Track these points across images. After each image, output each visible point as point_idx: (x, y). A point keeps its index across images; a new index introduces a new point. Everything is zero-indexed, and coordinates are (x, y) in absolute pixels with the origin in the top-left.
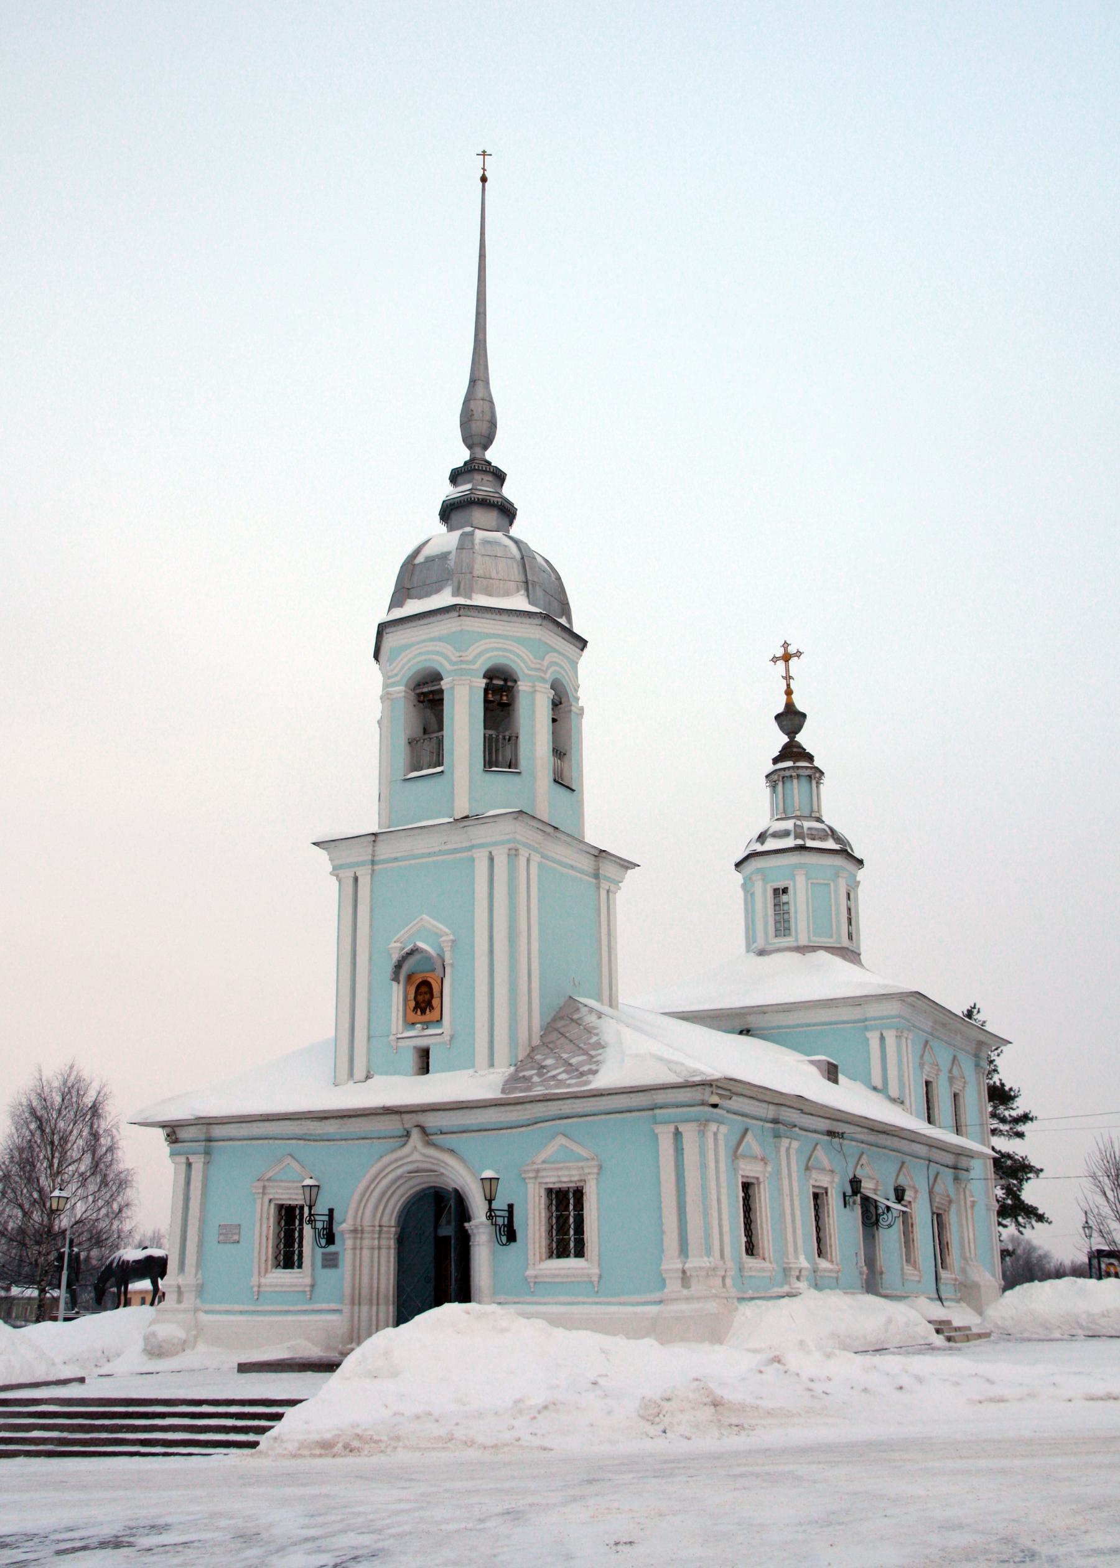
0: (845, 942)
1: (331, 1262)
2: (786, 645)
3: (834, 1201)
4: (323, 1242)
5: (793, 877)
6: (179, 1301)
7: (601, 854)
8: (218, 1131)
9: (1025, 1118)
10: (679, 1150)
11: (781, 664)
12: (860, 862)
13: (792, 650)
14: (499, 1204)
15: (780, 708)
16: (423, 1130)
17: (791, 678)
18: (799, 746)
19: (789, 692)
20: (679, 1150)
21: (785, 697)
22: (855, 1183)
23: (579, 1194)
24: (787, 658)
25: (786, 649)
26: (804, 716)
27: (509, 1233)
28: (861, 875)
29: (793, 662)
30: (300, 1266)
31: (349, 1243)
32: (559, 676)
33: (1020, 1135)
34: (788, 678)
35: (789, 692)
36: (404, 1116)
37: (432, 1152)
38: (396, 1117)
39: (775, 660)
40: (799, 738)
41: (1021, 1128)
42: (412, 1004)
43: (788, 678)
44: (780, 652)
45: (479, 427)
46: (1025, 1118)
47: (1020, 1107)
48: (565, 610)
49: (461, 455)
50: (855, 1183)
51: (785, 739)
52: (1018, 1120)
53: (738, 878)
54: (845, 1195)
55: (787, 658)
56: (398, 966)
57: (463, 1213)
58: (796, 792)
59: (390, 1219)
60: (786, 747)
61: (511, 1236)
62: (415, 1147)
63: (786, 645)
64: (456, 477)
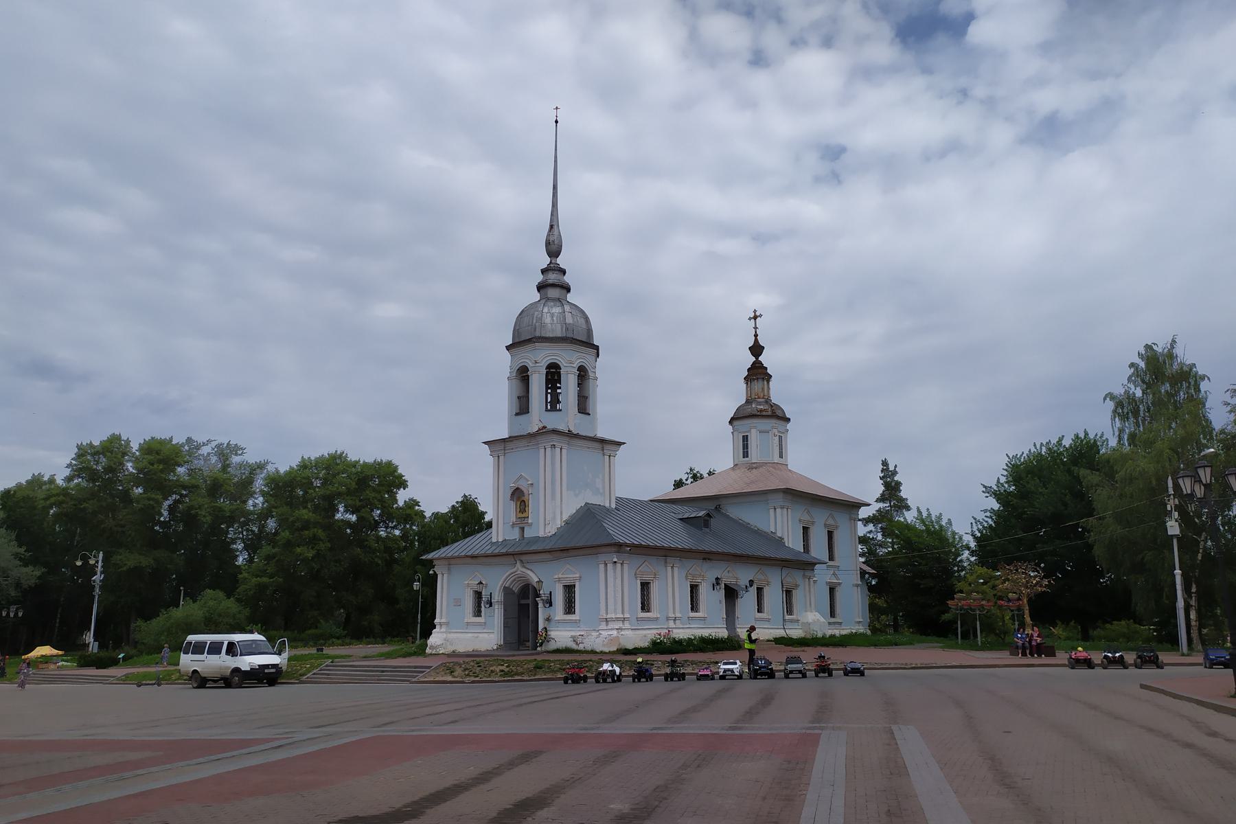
0: (776, 459)
2: (755, 311)
4: (488, 606)
5: (750, 431)
6: (441, 628)
7: (603, 441)
8: (453, 561)
10: (606, 570)
11: (753, 320)
12: (788, 420)
13: (758, 314)
15: (751, 344)
16: (521, 561)
17: (757, 328)
18: (761, 363)
19: (756, 336)
20: (606, 570)
21: (754, 338)
24: (755, 318)
25: (755, 313)
27: (550, 603)
28: (789, 426)
31: (496, 607)
32: (583, 364)
34: (756, 328)
35: (756, 336)
36: (515, 556)
37: (524, 570)
38: (512, 556)
39: (750, 319)
40: (760, 359)
42: (518, 510)
43: (756, 328)
45: (554, 248)
48: (589, 332)
49: (545, 261)
51: (754, 359)
54: (713, 585)
55: (755, 318)
56: (513, 494)
58: (756, 387)
60: (754, 363)
61: (551, 605)
62: (518, 569)
63: (755, 311)
64: (543, 271)
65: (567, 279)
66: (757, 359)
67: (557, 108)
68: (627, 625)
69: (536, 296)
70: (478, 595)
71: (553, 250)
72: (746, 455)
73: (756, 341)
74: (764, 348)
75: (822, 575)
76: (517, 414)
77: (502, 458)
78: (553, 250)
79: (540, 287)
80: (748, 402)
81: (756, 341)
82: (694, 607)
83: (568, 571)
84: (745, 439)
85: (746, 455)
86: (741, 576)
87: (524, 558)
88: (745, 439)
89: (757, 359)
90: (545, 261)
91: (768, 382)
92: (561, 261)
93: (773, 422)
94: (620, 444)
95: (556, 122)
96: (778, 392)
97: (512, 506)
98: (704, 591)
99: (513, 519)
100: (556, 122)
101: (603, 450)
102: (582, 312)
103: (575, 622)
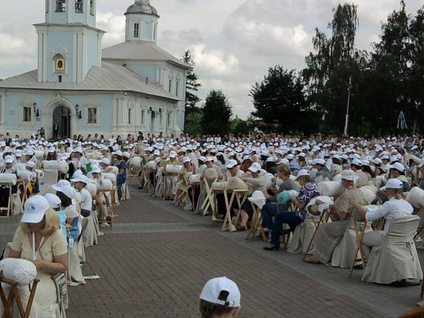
1: (38, 120)
3: (146, 112)
7: (99, 31)
12: (159, 17)
14: (79, 111)
22: (151, 108)
23: (95, 110)
30: (30, 120)
33: (196, 90)
41: (197, 88)
47: (197, 82)
50: (151, 108)
52: (196, 85)
57: (69, 111)
59: (51, 111)
61: (80, 117)
70: (27, 110)
72: (136, 34)
76: (56, 11)
77: (45, 35)
83: (92, 101)
84: (137, 26)
85: (136, 34)
86: (156, 106)
87: (62, 92)
88: (137, 26)
94: (105, 32)
97: (54, 65)
99: (54, 71)
101: (98, 35)
103: (97, 127)
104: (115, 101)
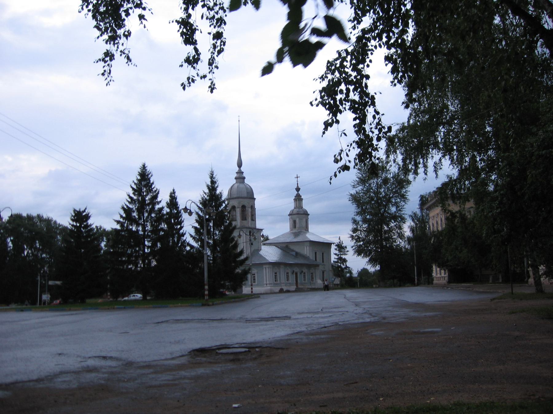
2: (297, 175)
9: (348, 251)
11: (296, 178)
12: (309, 214)
13: (298, 176)
15: (296, 187)
19: (298, 184)
24: (297, 177)
26: (300, 189)
28: (309, 217)
29: (298, 178)
34: (297, 181)
35: (298, 184)
39: (295, 178)
41: (347, 253)
43: (297, 181)
44: (296, 176)
46: (348, 251)
51: (297, 192)
53: (289, 217)
55: (297, 177)
60: (297, 194)
63: (297, 175)
65: (244, 175)
66: (298, 192)
67: (239, 116)
68: (272, 285)
69: (235, 181)
71: (240, 165)
73: (298, 186)
74: (300, 189)
75: (321, 268)
78: (240, 165)
79: (236, 178)
80: (295, 208)
81: (298, 186)
82: (288, 280)
88: (295, 222)
89: (298, 192)
90: (238, 169)
91: (302, 201)
92: (242, 169)
93: (304, 216)
95: (239, 121)
96: (306, 206)
98: (290, 274)
100: (239, 121)
102: (250, 187)
104: (264, 269)
